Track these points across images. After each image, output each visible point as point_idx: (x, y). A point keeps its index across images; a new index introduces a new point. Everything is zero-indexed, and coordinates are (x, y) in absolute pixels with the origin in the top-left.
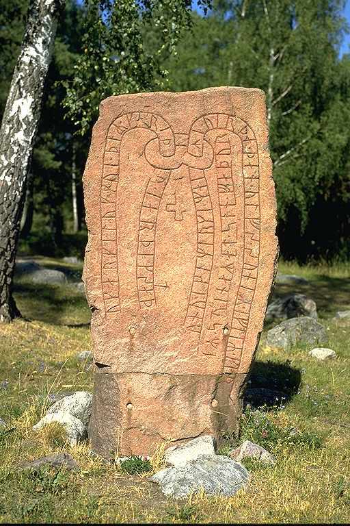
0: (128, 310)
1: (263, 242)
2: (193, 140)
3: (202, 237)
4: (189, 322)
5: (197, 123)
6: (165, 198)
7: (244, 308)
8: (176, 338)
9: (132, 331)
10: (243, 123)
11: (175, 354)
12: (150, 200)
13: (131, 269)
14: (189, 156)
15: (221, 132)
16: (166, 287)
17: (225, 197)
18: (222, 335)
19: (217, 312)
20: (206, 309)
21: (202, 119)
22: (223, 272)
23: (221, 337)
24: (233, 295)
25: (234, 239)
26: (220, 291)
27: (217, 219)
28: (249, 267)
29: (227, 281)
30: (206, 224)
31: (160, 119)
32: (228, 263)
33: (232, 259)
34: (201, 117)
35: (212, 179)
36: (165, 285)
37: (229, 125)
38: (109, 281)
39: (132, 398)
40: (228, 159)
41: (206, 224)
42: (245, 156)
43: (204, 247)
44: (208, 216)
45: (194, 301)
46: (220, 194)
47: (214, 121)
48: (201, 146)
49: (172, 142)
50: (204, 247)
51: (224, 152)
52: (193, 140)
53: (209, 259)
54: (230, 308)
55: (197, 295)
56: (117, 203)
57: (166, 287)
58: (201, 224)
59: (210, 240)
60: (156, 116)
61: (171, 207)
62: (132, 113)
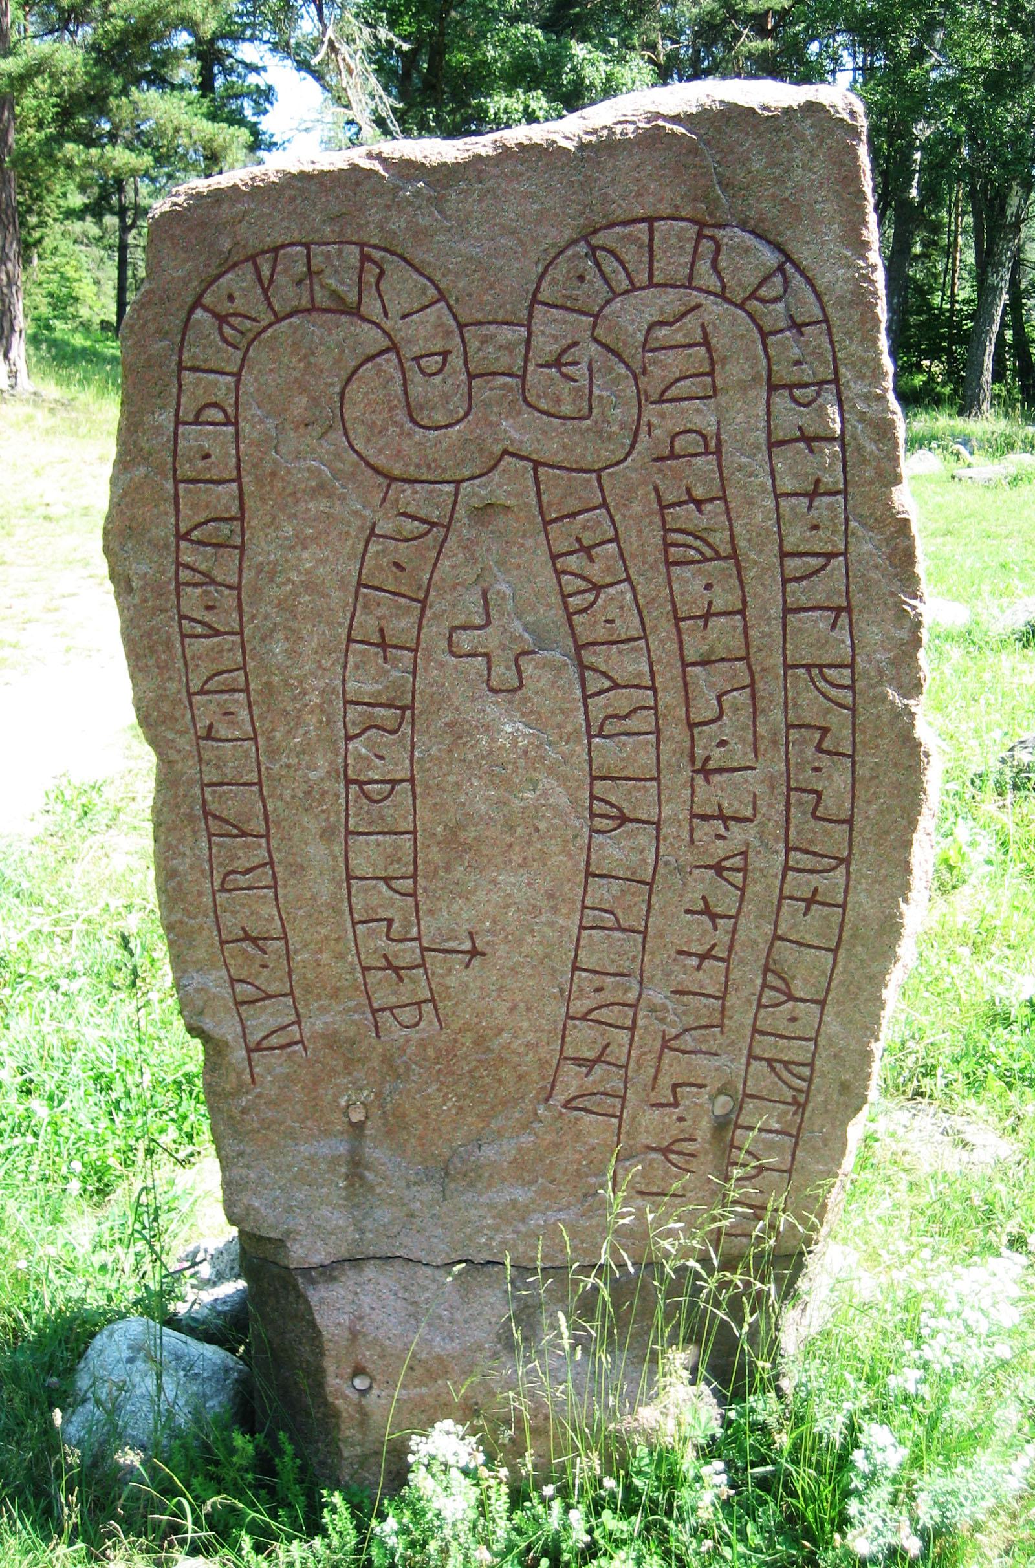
0: (331, 1040)
1: (868, 761)
2: (545, 347)
3: (609, 752)
4: (572, 1081)
5: (560, 271)
6: (438, 603)
7: (793, 1019)
8: (526, 1140)
9: (357, 1116)
10: (770, 258)
11: (521, 1195)
12: (380, 612)
13: (325, 889)
14: (527, 415)
15: (670, 301)
16: (474, 952)
17: (698, 585)
18: (705, 1124)
19: (688, 1041)
20: (638, 1033)
21: (582, 248)
22: (701, 884)
23: (705, 1126)
24: (748, 976)
25: (740, 753)
26: (694, 961)
27: (668, 676)
28: (807, 861)
29: (720, 922)
30: (622, 700)
31: (392, 265)
32: (720, 849)
33: (738, 834)
34: (574, 242)
35: (636, 508)
36: (467, 946)
37: (704, 266)
38: (247, 937)
39: (368, 1356)
40: (704, 417)
41: (622, 700)
42: (781, 401)
43: (616, 793)
44: (632, 666)
45: (589, 1003)
46: (676, 570)
47: (630, 254)
48: (584, 366)
49: (456, 361)
50: (616, 793)
51: (683, 388)
52: (545, 347)
53: (645, 837)
54: (741, 1016)
55: (598, 981)
56: (246, 632)
57: (474, 952)
58: (601, 700)
59: (645, 761)
60: (377, 255)
61: (465, 641)
62: (276, 250)
